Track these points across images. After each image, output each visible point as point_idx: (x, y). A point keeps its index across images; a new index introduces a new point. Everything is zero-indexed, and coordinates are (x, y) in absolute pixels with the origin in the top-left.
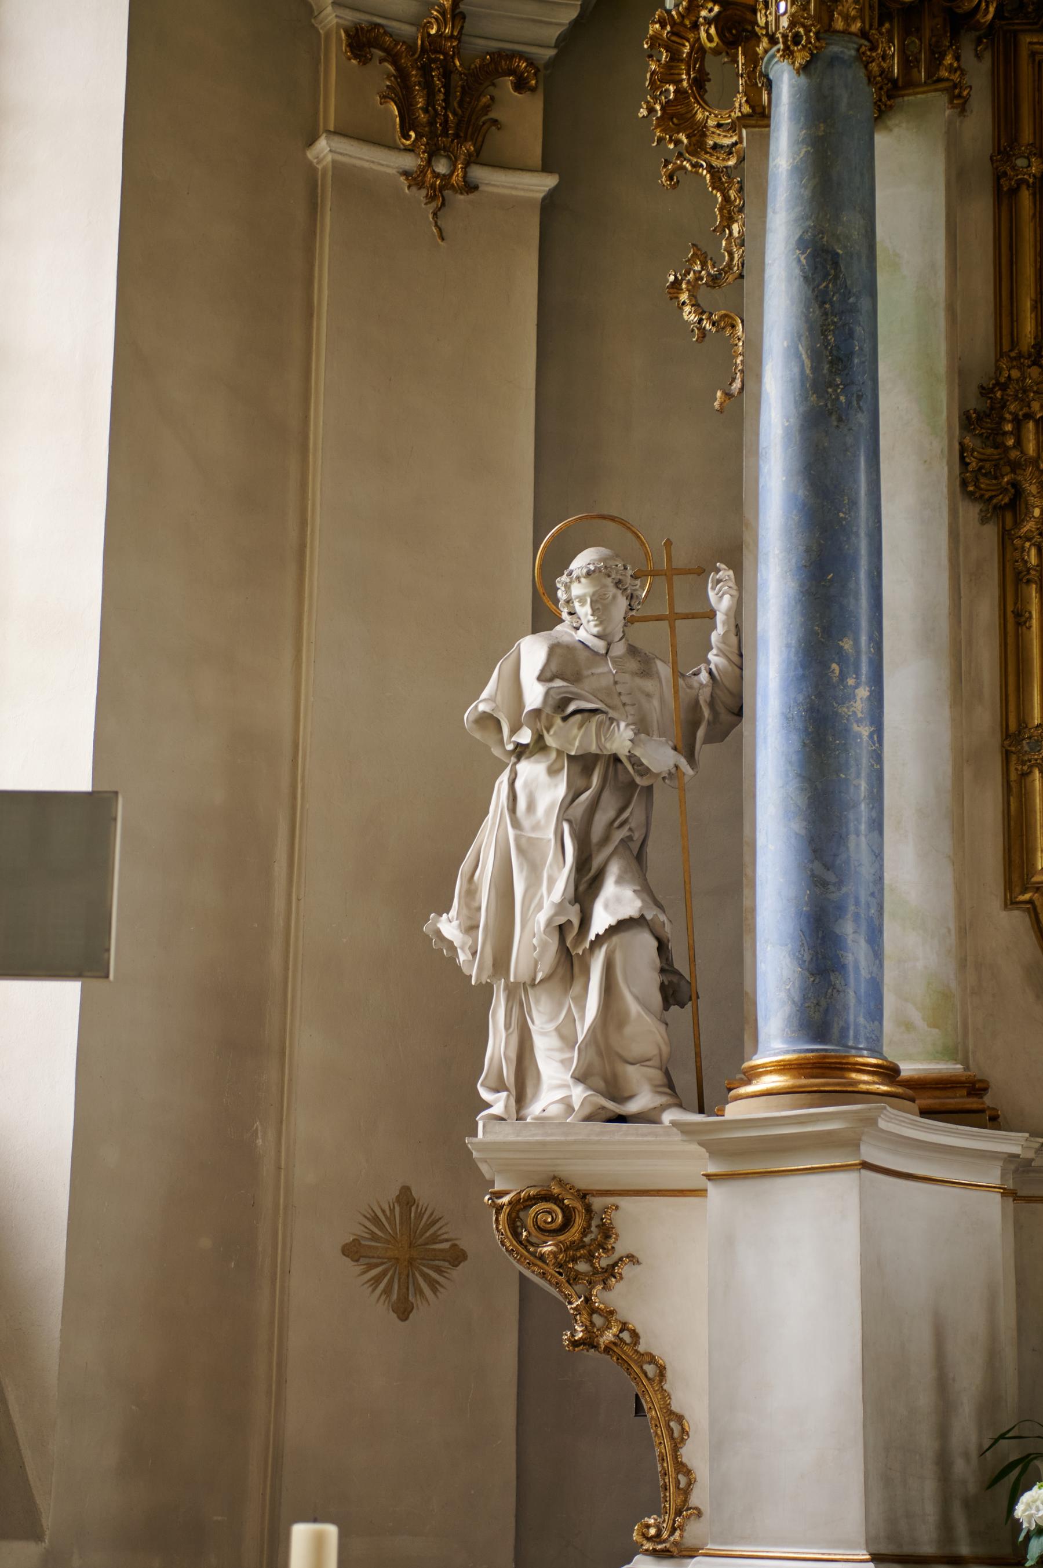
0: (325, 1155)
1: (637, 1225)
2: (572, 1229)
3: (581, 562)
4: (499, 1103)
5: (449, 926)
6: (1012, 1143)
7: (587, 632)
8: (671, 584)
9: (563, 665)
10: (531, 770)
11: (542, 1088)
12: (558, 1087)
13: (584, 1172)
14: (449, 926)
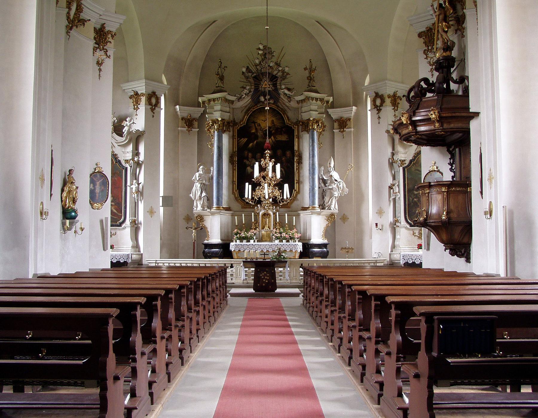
0: (182, 212)
1: (205, 218)
2: (201, 218)
3: (201, 167)
4: (195, 209)
5: (191, 195)
6: (231, 212)
7: (201, 173)
8: (207, 171)
9: (200, 175)
10: (197, 183)
11: (198, 208)
12: (199, 208)
13: (201, 214)
14: (191, 195)
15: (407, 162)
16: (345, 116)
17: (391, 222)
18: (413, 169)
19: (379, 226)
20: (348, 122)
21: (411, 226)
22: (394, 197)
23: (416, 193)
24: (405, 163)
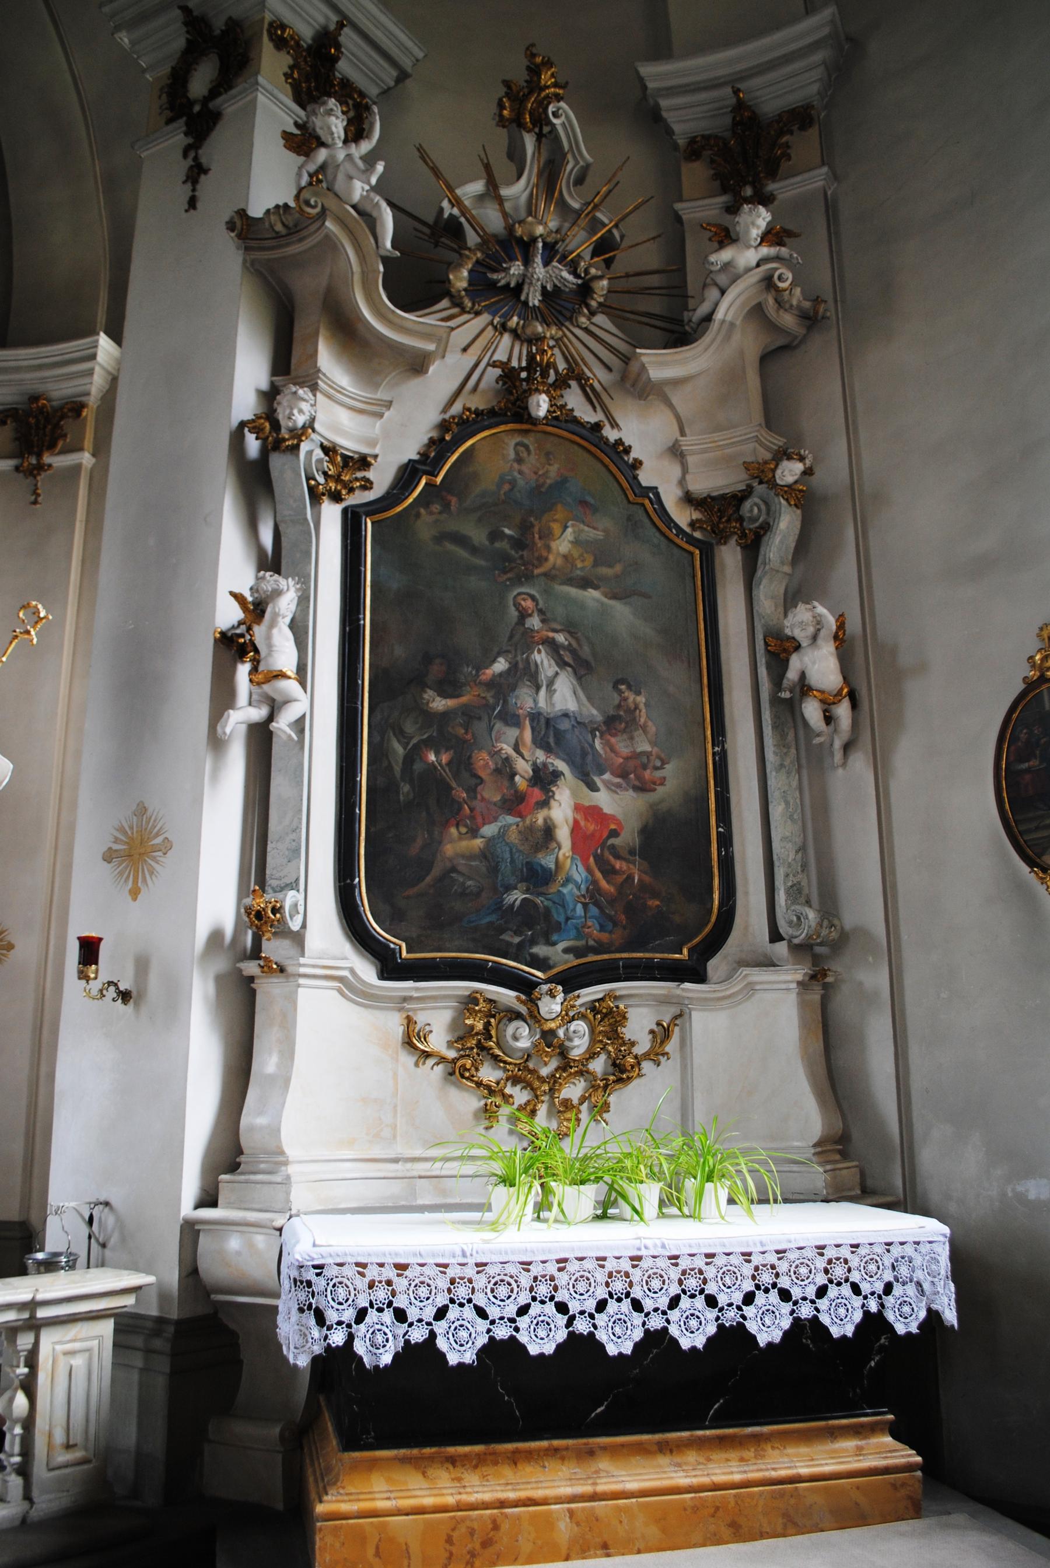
15: (381, 478)
16: (59, 390)
17: (215, 937)
18: (425, 527)
19: (106, 967)
20: (67, 425)
21: (390, 968)
22: (258, 714)
23: (439, 704)
24: (367, 485)
